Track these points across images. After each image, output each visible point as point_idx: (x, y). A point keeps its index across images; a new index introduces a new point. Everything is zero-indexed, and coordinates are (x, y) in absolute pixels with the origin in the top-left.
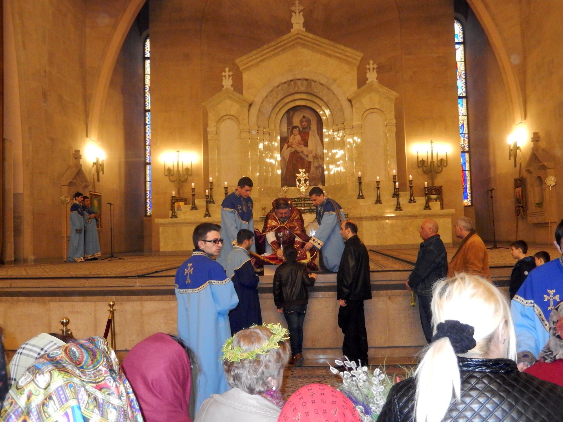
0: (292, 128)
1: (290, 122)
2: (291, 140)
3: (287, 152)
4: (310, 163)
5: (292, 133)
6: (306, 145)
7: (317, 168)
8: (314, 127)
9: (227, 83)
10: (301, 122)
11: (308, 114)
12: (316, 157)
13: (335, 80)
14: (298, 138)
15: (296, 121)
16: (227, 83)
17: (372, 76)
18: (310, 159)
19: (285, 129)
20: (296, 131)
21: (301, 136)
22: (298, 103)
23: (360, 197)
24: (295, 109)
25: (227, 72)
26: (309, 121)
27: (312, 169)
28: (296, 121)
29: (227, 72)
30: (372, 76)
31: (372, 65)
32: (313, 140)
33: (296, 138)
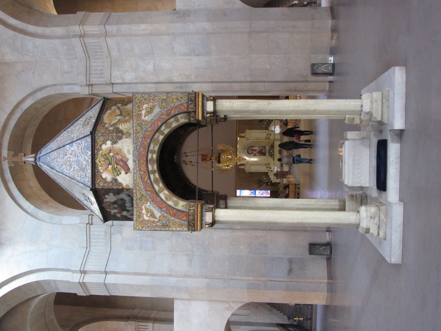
0: (252, 153)
1: (251, 154)
2: (254, 153)
3: (258, 154)
4: (261, 149)
5: (253, 153)
6: (256, 150)
7: (262, 148)
8: (252, 148)
9: (242, 167)
10: (251, 151)
11: (249, 149)
12: (259, 148)
13: (243, 143)
14: (254, 152)
15: (250, 152)
16: (242, 167)
17: (243, 135)
18: (260, 149)
19: (252, 155)
20: (253, 152)
21: (255, 151)
22: (247, 152)
23: (269, 138)
24: (248, 152)
25: (240, 167)
26: (251, 149)
27: (262, 149)
28: (250, 152)
29: (240, 167)
30: (243, 135)
31: (240, 135)
32: (255, 148)
33: (255, 152)
